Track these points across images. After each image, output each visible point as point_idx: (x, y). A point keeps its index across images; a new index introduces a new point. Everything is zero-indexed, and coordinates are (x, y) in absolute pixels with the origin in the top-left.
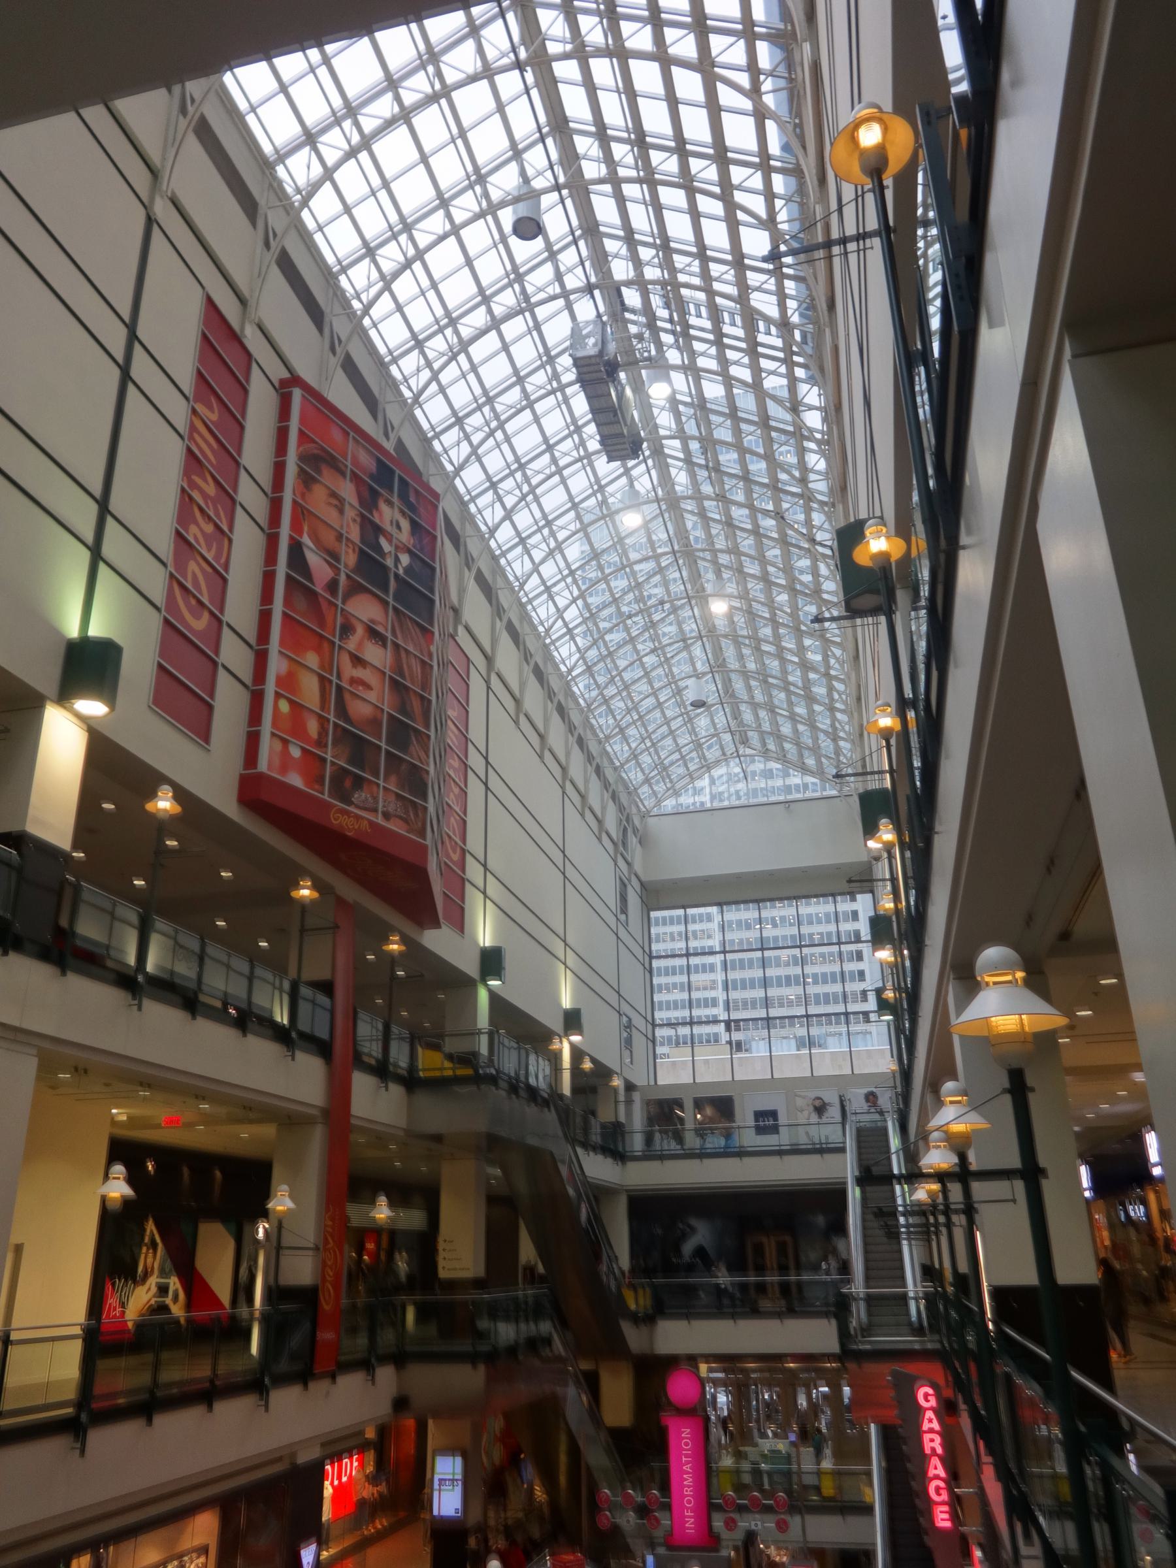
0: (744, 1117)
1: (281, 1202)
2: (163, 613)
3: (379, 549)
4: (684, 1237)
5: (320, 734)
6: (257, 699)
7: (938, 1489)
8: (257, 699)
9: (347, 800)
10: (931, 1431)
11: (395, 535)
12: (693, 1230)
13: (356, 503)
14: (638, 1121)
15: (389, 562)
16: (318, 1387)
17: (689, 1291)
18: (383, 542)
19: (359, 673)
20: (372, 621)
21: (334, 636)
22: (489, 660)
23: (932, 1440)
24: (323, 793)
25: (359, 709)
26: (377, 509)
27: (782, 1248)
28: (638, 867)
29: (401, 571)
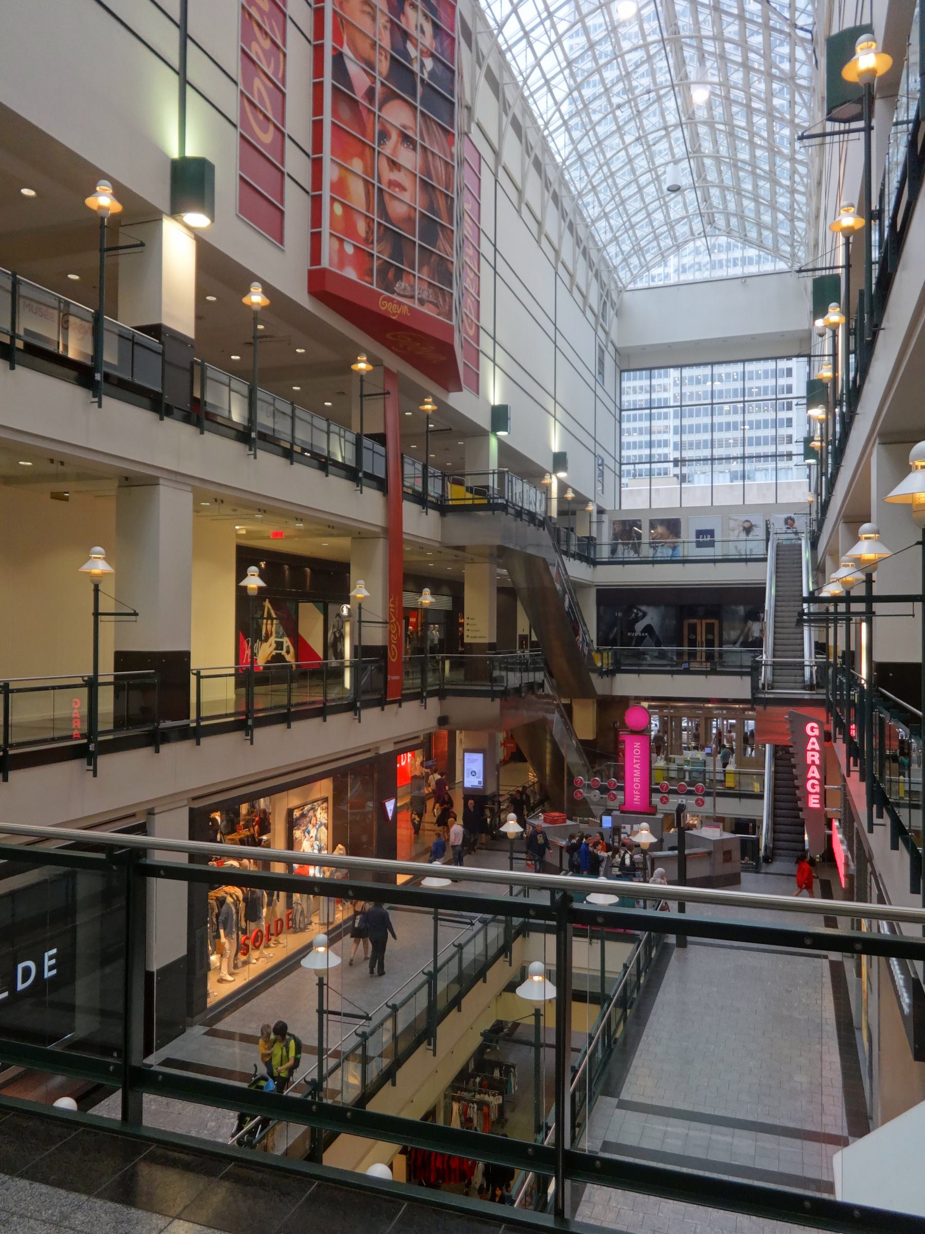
0: (688, 534)
1: (359, 592)
2: (239, 129)
3: (406, 55)
4: (637, 620)
5: (367, 233)
6: (316, 202)
7: (813, 786)
8: (316, 202)
9: (390, 288)
10: (813, 750)
11: (420, 40)
12: (645, 615)
13: (386, 11)
14: (605, 536)
15: (416, 68)
16: (391, 709)
17: (640, 655)
18: (410, 46)
19: (396, 176)
20: (404, 127)
21: (374, 143)
22: (497, 154)
23: (813, 756)
24: (372, 284)
25: (397, 209)
26: (404, 14)
27: (710, 629)
28: (614, 335)
29: (426, 76)
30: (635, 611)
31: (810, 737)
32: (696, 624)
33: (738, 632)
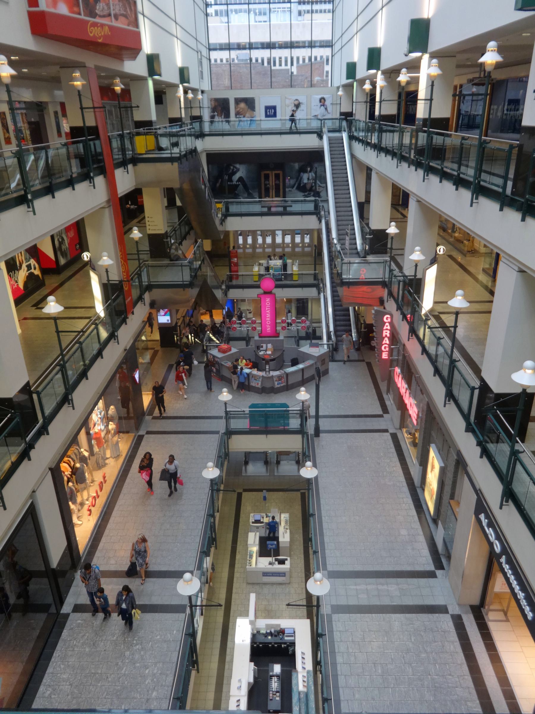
4: (234, 173)
7: (385, 348)
9: (93, 14)
10: (387, 329)
12: (238, 170)
24: (80, 14)
27: (277, 176)
30: (232, 167)
31: (385, 323)
33: (295, 180)
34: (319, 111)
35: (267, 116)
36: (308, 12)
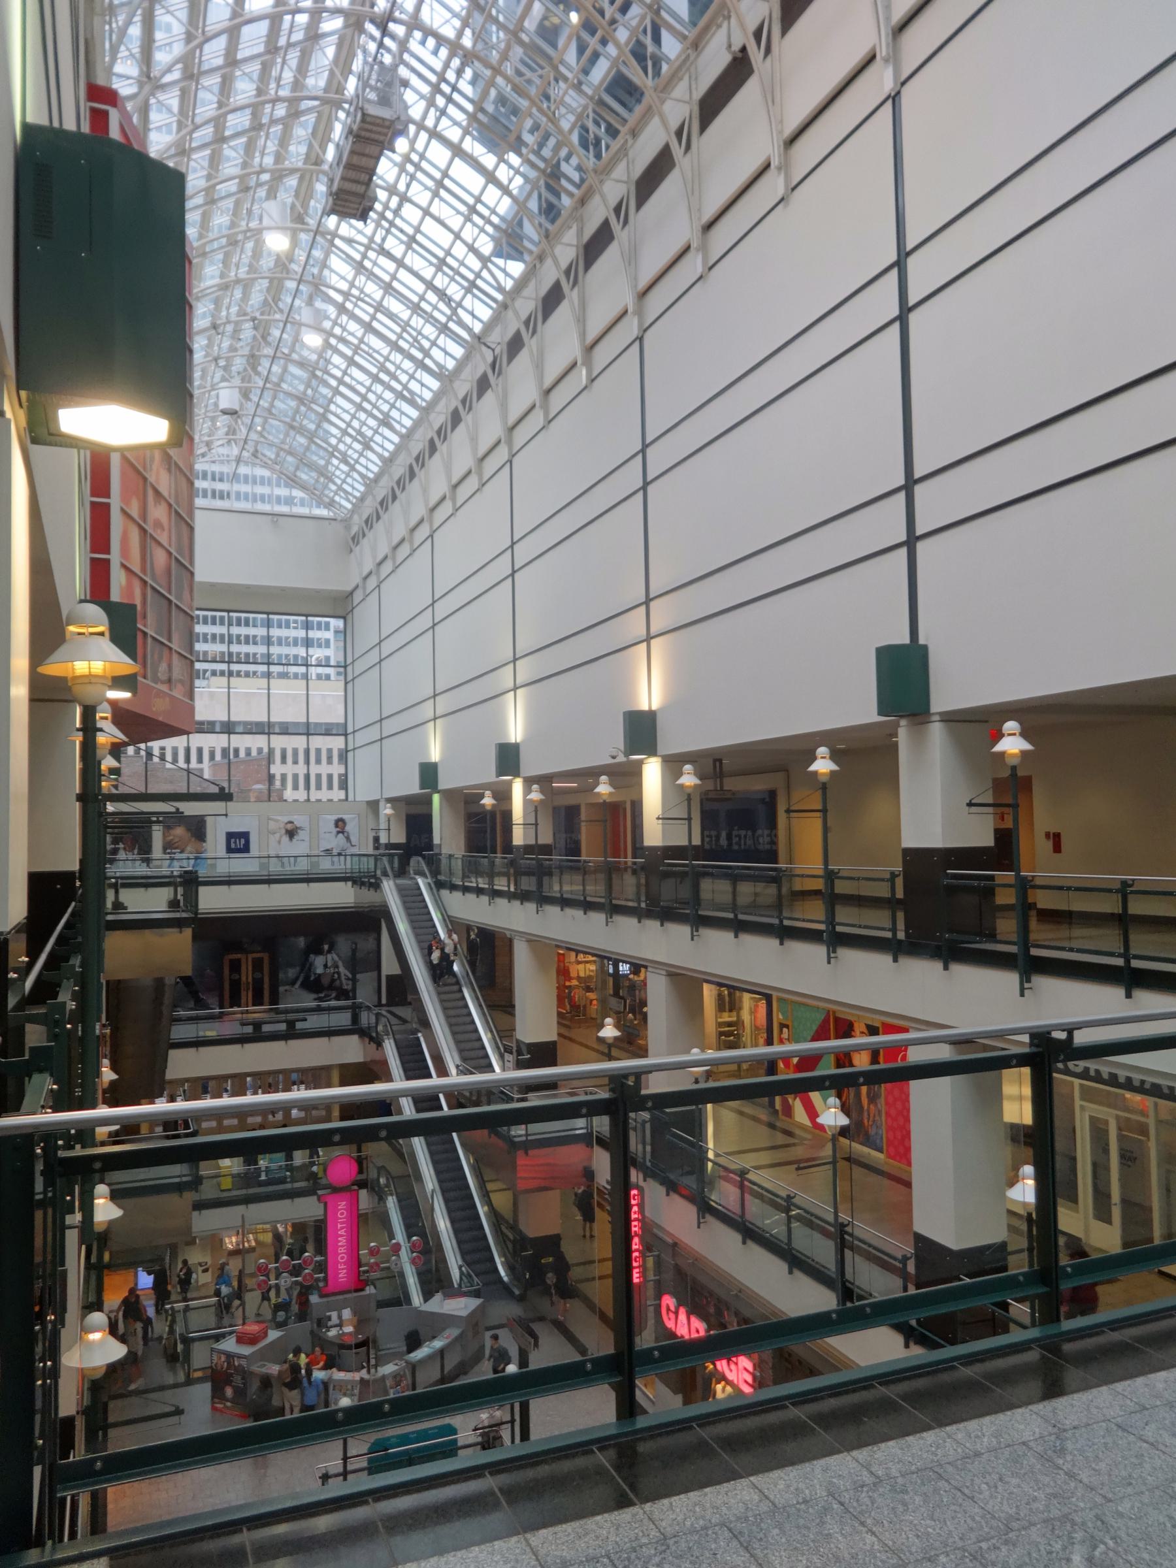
27: (258, 965)
32: (239, 961)
33: (298, 969)
34: (335, 842)
35: (229, 850)
36: (222, 673)
